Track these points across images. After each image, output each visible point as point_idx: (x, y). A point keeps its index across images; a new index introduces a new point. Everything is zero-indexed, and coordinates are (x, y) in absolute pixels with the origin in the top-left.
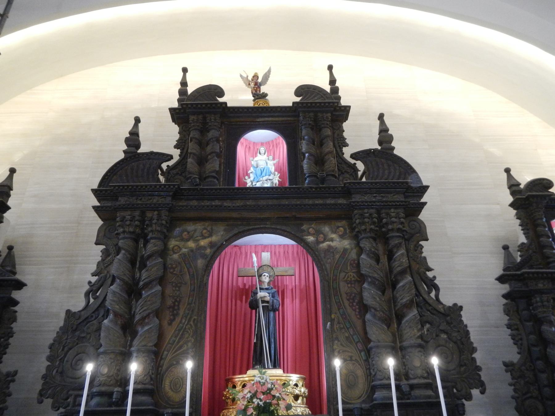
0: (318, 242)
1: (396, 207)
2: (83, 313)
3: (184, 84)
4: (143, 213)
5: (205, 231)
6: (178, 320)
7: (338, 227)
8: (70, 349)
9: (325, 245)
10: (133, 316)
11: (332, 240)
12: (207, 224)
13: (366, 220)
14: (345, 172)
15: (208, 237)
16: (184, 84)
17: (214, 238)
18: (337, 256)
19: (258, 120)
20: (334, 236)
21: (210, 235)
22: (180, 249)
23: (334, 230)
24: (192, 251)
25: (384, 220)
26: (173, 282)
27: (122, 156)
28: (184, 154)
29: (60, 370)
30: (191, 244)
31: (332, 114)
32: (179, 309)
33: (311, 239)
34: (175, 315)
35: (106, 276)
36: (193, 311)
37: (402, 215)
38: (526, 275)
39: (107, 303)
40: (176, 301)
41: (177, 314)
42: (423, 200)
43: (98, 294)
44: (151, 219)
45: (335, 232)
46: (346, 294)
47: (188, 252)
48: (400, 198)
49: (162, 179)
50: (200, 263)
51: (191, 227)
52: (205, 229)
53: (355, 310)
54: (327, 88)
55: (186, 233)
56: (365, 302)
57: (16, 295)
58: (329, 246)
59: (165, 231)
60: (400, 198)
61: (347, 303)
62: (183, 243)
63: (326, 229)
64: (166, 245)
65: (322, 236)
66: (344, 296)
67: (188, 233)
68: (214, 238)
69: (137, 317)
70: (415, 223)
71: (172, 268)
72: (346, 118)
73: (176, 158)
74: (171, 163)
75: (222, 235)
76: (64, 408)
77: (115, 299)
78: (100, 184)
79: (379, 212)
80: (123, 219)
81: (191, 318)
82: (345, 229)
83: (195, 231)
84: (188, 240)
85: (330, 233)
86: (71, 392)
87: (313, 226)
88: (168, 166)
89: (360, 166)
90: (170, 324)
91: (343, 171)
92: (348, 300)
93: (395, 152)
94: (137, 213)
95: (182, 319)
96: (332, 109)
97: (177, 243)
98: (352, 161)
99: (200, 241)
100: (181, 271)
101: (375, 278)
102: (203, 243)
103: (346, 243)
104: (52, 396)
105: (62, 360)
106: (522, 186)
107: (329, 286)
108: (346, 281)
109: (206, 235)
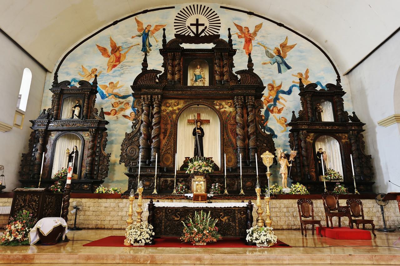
0: (220, 109)
1: (251, 95)
2: (131, 134)
3: (164, 36)
4: (151, 97)
5: (176, 103)
6: (166, 137)
7: (228, 103)
8: (128, 146)
9: (223, 110)
10: (150, 135)
11: (226, 108)
12: (176, 100)
13: (239, 101)
14: (233, 79)
15: (177, 106)
16: (164, 36)
17: (179, 106)
18: (227, 114)
19: (197, 55)
20: (226, 106)
21: (178, 105)
22: (166, 110)
23: (227, 104)
24: (171, 111)
25: (247, 101)
26: (164, 123)
27: (141, 72)
28: (166, 70)
29: (126, 153)
30: (170, 109)
31: (228, 53)
32: (167, 133)
33: (217, 107)
34: (165, 136)
35: (139, 120)
36: (172, 134)
37: (253, 99)
38: (298, 123)
39: (141, 131)
40: (165, 130)
41: (166, 135)
42: (262, 93)
43: (136, 127)
44: (155, 99)
45: (227, 105)
46: (230, 129)
47: (169, 112)
48: (253, 92)
49: (157, 80)
50: (174, 116)
51: (170, 101)
52: (175, 102)
53: (233, 135)
54: (227, 40)
55: (168, 104)
56: (237, 132)
57: (106, 126)
58: (225, 110)
59: (160, 103)
60: (253, 92)
61: (230, 132)
62: (167, 108)
63: (224, 103)
64: (160, 108)
65: (222, 106)
66: (229, 130)
67: (169, 104)
68: (179, 106)
69: (152, 136)
70: (259, 102)
71: (163, 118)
72: (235, 54)
73: (163, 72)
74: (161, 74)
75: (182, 105)
76: (129, 166)
77: (144, 129)
78: (134, 84)
79: (245, 98)
80: (144, 98)
81: (171, 137)
82: (231, 104)
83: (172, 103)
84: (169, 107)
85: (225, 105)
86: (130, 161)
87: (218, 102)
88: (159, 75)
89: (239, 77)
90: (164, 138)
91: (232, 79)
92: (231, 131)
93: (254, 71)
94: (149, 96)
95: (168, 137)
96: (228, 51)
97: (165, 108)
98: (236, 75)
99: (174, 107)
100: (167, 119)
101: (241, 123)
102: (175, 108)
103: (231, 109)
104: (124, 162)
105: (126, 150)
106: (305, 87)
107: (223, 126)
108: (230, 124)
109: (176, 105)
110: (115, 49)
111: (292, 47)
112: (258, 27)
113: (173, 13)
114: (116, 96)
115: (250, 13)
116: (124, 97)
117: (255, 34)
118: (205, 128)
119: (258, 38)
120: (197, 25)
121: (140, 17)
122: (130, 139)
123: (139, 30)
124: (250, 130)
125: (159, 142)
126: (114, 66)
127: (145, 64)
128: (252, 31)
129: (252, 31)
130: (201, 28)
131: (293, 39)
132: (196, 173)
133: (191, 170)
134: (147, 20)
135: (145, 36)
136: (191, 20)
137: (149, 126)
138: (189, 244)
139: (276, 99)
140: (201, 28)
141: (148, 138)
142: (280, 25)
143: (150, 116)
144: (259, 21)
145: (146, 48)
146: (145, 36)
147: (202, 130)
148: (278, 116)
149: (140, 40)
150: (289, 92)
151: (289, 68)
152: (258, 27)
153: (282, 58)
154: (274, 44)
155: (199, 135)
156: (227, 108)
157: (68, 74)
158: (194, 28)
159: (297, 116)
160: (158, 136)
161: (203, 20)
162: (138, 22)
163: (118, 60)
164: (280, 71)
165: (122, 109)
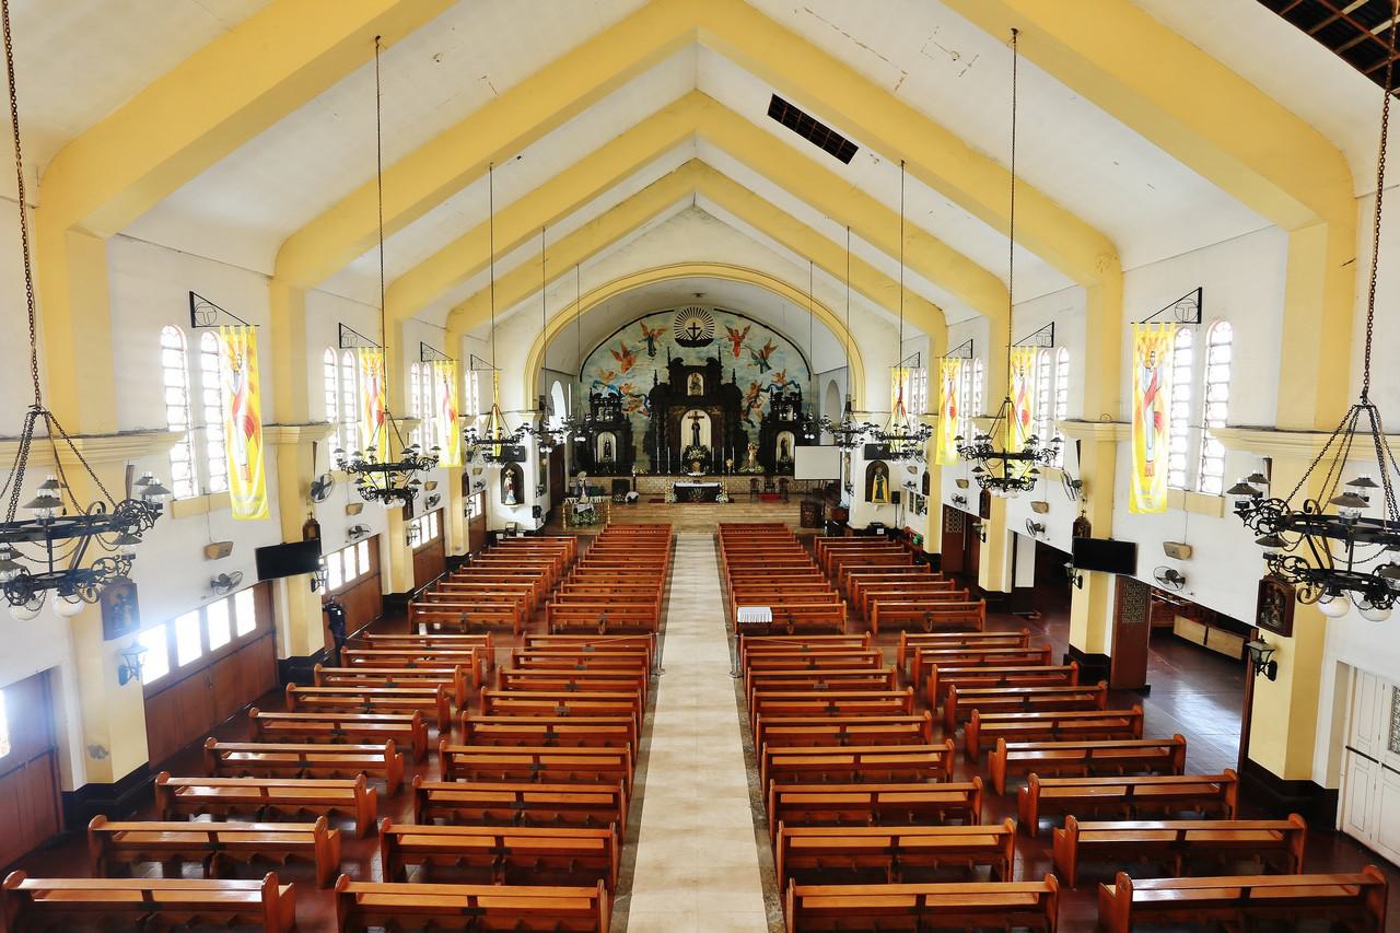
110: (627, 353)
111: (774, 348)
112: (747, 330)
113: (673, 317)
114: (632, 395)
115: (740, 316)
116: (638, 396)
117: (743, 337)
118: (700, 421)
119: (745, 340)
120: (694, 328)
121: (646, 321)
122: (649, 436)
123: (644, 334)
124: (731, 429)
125: (669, 439)
126: (627, 369)
127: (656, 379)
128: (741, 334)
129: (741, 334)
130: (697, 332)
131: (777, 339)
132: (695, 460)
133: (691, 457)
134: (653, 324)
135: (650, 339)
136: (688, 324)
137: (662, 428)
138: (692, 501)
139: (758, 396)
140: (697, 332)
141: (662, 436)
142: (766, 327)
143: (662, 419)
144: (748, 323)
145: (652, 352)
146: (650, 339)
147: (698, 425)
148: (756, 409)
149: (646, 344)
150: (767, 391)
151: (770, 368)
152: (747, 330)
153: (765, 359)
154: (759, 346)
155: (696, 428)
156: (716, 412)
157: (590, 377)
158: (691, 332)
159: (766, 415)
160: (668, 435)
161: (700, 323)
162: (643, 326)
163: (630, 363)
164: (762, 372)
165: (637, 406)
